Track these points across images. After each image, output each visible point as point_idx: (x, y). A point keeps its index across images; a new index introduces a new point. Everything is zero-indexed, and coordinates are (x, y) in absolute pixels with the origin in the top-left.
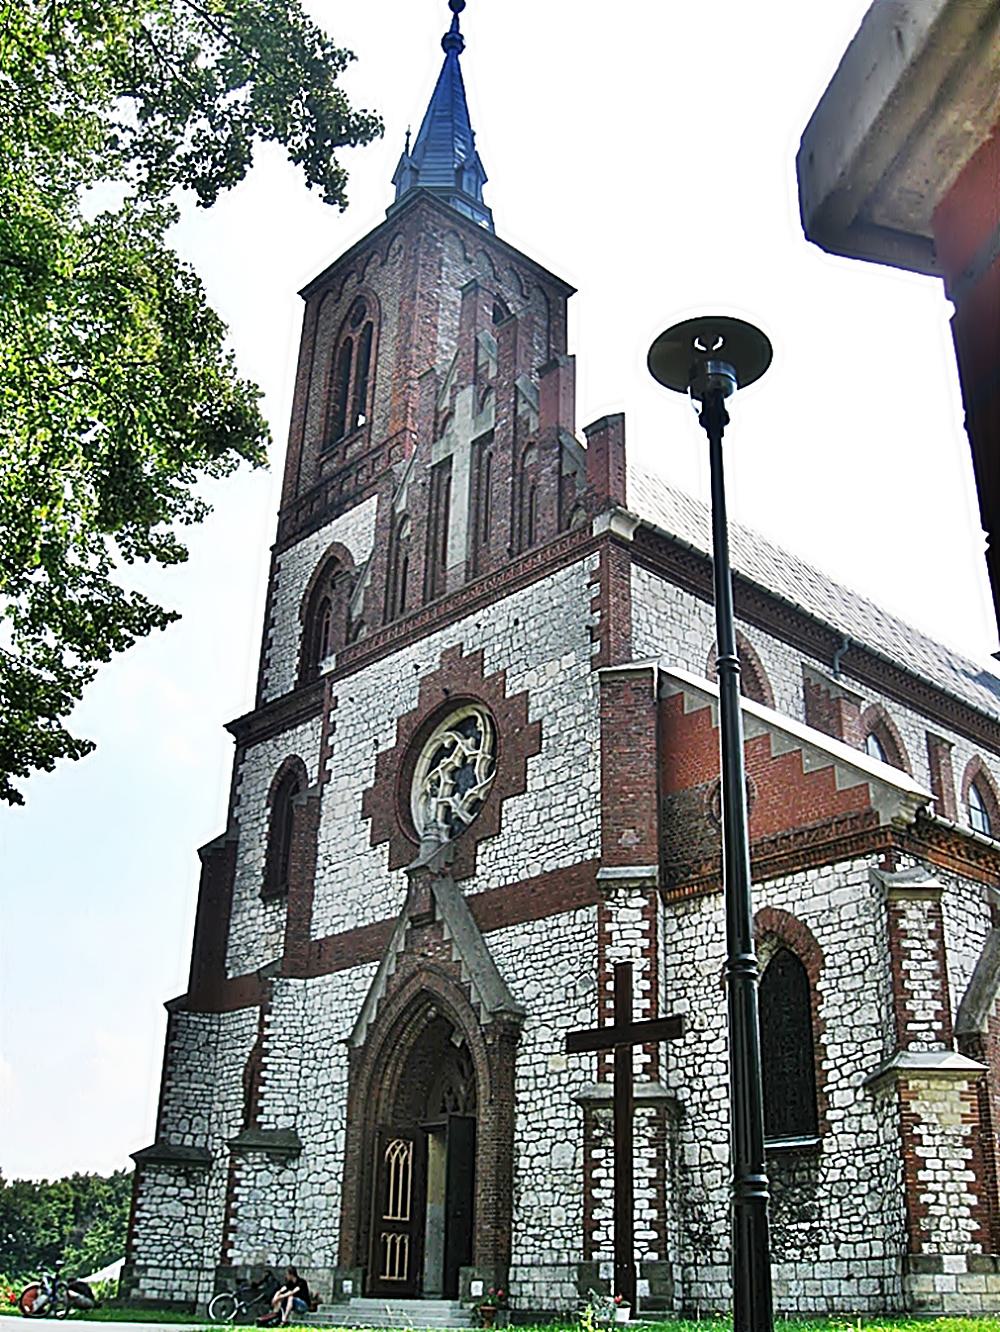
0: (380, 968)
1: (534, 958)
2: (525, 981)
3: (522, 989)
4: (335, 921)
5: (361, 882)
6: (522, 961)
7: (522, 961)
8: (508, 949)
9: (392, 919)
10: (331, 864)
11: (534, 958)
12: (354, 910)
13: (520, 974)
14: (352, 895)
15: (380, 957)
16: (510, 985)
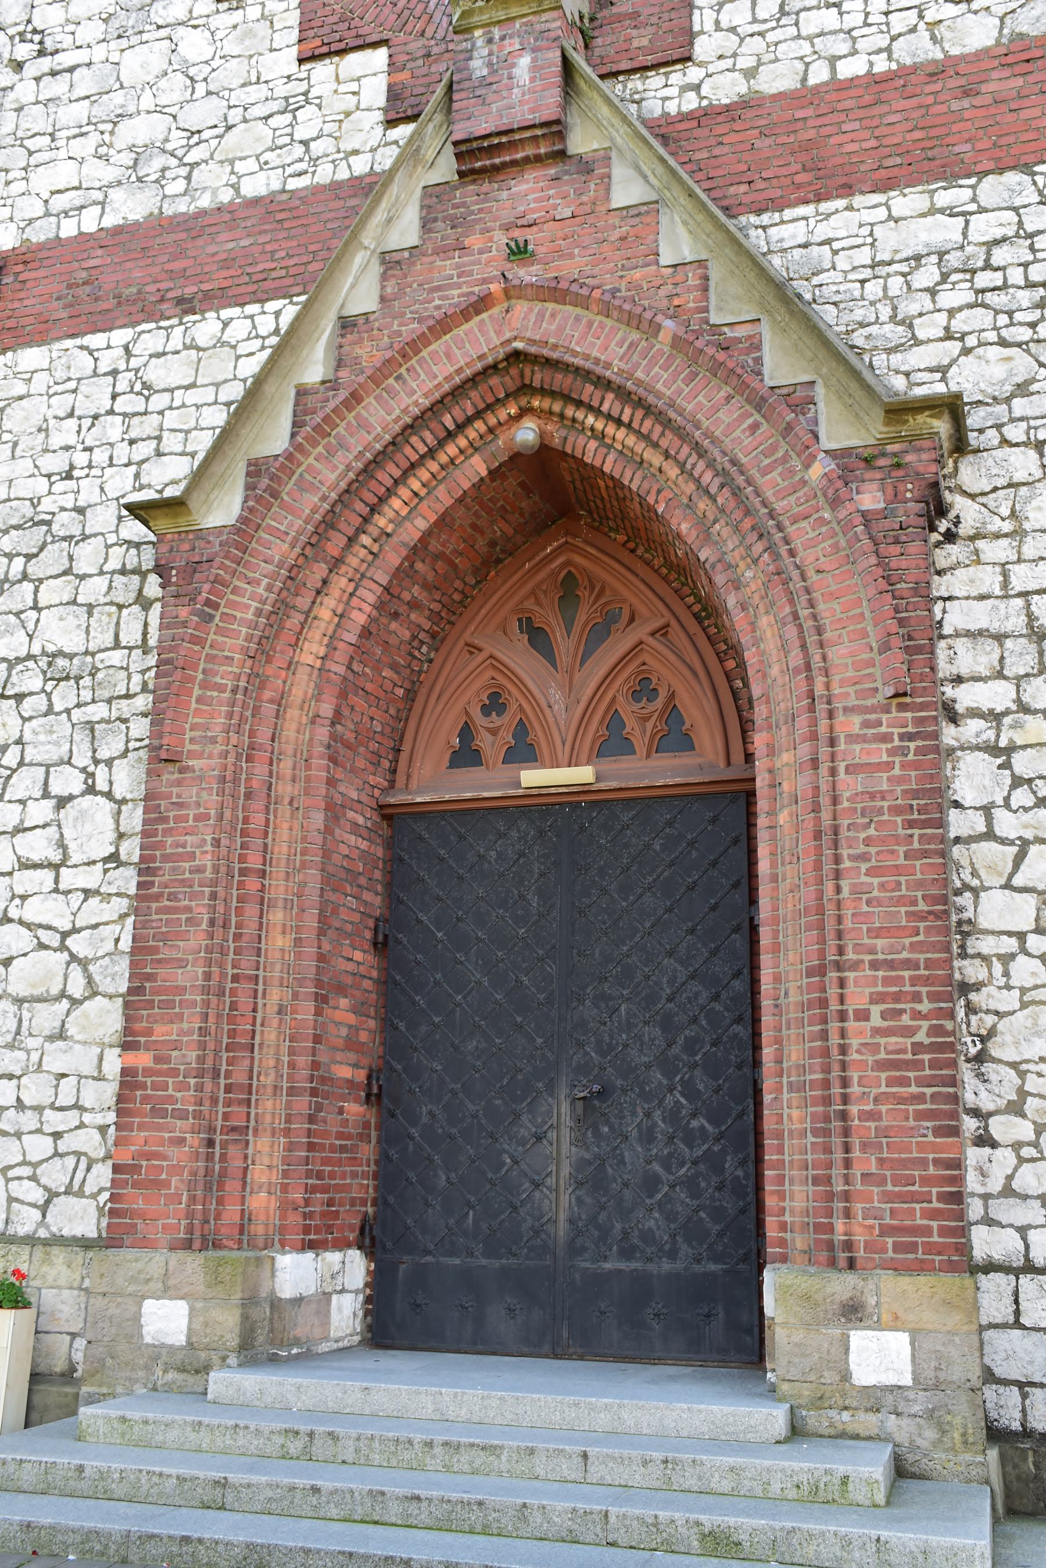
0: (306, 306)
1: (984, 279)
2: (955, 347)
3: (943, 370)
4: (59, 203)
5: (176, 97)
6: (932, 292)
7: (932, 292)
8: (864, 256)
9: (317, 190)
10: (41, 53)
11: (984, 279)
12: (152, 168)
13: (929, 328)
14: (139, 130)
15: (307, 277)
16: (880, 360)
